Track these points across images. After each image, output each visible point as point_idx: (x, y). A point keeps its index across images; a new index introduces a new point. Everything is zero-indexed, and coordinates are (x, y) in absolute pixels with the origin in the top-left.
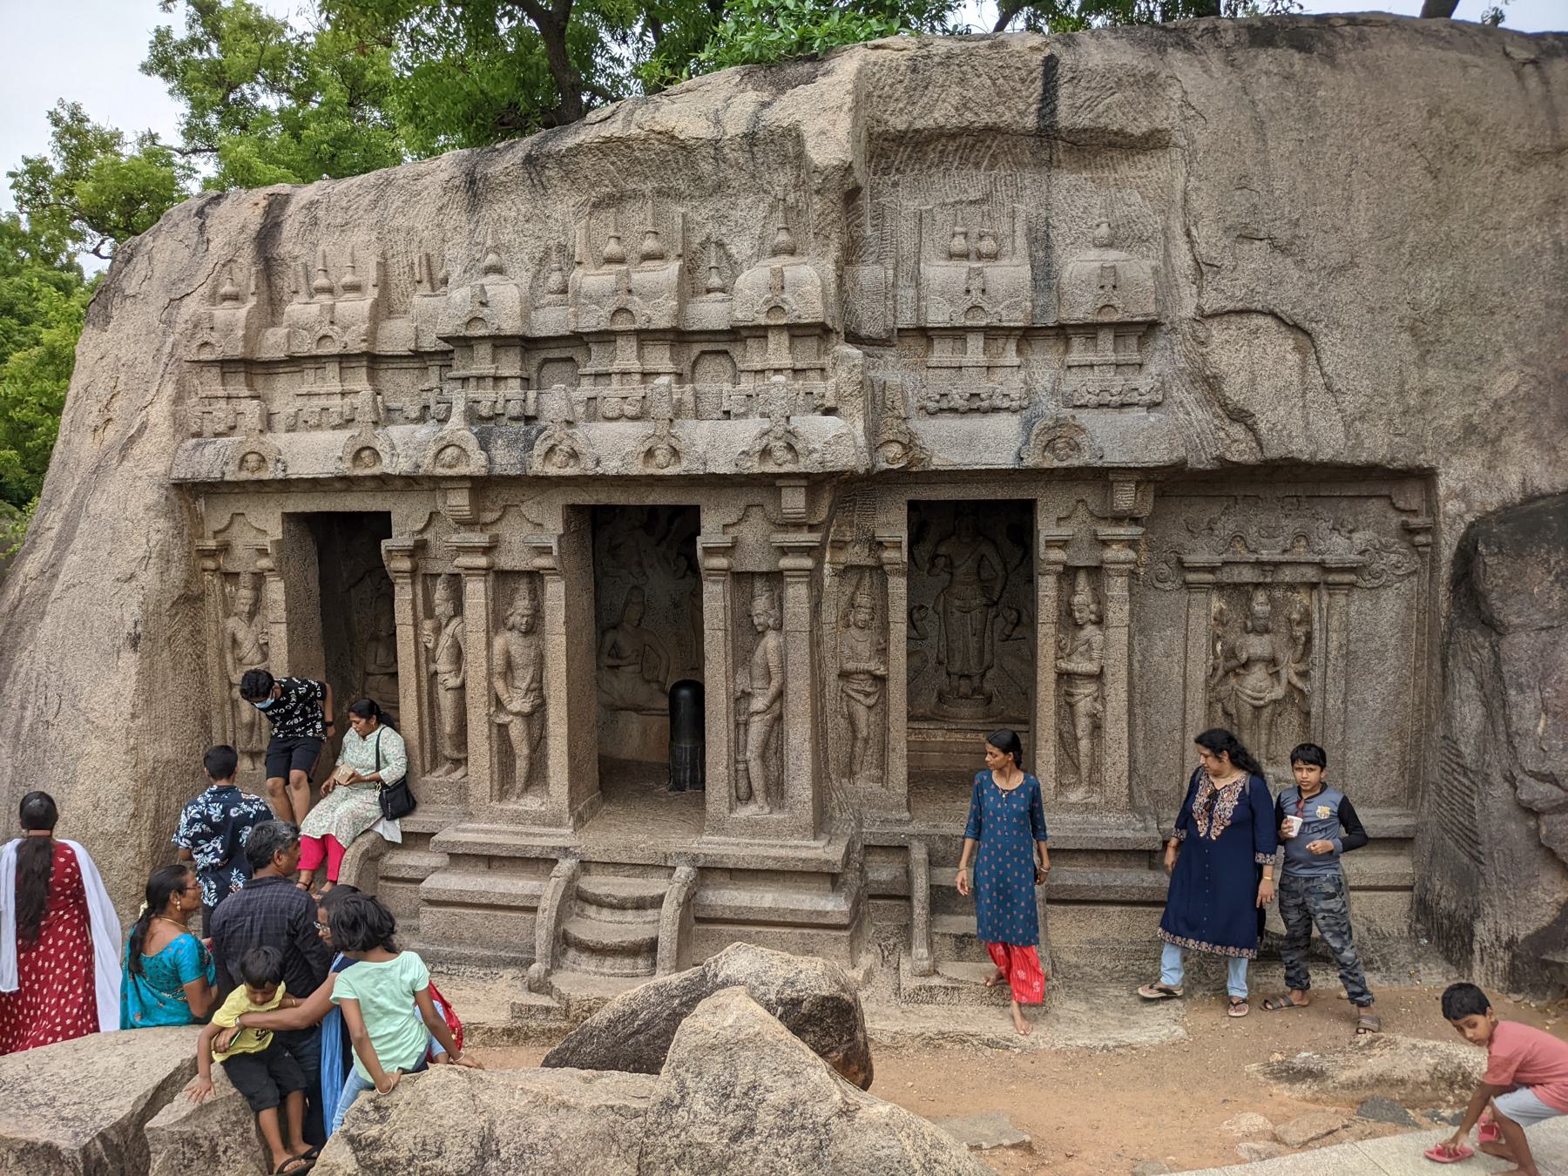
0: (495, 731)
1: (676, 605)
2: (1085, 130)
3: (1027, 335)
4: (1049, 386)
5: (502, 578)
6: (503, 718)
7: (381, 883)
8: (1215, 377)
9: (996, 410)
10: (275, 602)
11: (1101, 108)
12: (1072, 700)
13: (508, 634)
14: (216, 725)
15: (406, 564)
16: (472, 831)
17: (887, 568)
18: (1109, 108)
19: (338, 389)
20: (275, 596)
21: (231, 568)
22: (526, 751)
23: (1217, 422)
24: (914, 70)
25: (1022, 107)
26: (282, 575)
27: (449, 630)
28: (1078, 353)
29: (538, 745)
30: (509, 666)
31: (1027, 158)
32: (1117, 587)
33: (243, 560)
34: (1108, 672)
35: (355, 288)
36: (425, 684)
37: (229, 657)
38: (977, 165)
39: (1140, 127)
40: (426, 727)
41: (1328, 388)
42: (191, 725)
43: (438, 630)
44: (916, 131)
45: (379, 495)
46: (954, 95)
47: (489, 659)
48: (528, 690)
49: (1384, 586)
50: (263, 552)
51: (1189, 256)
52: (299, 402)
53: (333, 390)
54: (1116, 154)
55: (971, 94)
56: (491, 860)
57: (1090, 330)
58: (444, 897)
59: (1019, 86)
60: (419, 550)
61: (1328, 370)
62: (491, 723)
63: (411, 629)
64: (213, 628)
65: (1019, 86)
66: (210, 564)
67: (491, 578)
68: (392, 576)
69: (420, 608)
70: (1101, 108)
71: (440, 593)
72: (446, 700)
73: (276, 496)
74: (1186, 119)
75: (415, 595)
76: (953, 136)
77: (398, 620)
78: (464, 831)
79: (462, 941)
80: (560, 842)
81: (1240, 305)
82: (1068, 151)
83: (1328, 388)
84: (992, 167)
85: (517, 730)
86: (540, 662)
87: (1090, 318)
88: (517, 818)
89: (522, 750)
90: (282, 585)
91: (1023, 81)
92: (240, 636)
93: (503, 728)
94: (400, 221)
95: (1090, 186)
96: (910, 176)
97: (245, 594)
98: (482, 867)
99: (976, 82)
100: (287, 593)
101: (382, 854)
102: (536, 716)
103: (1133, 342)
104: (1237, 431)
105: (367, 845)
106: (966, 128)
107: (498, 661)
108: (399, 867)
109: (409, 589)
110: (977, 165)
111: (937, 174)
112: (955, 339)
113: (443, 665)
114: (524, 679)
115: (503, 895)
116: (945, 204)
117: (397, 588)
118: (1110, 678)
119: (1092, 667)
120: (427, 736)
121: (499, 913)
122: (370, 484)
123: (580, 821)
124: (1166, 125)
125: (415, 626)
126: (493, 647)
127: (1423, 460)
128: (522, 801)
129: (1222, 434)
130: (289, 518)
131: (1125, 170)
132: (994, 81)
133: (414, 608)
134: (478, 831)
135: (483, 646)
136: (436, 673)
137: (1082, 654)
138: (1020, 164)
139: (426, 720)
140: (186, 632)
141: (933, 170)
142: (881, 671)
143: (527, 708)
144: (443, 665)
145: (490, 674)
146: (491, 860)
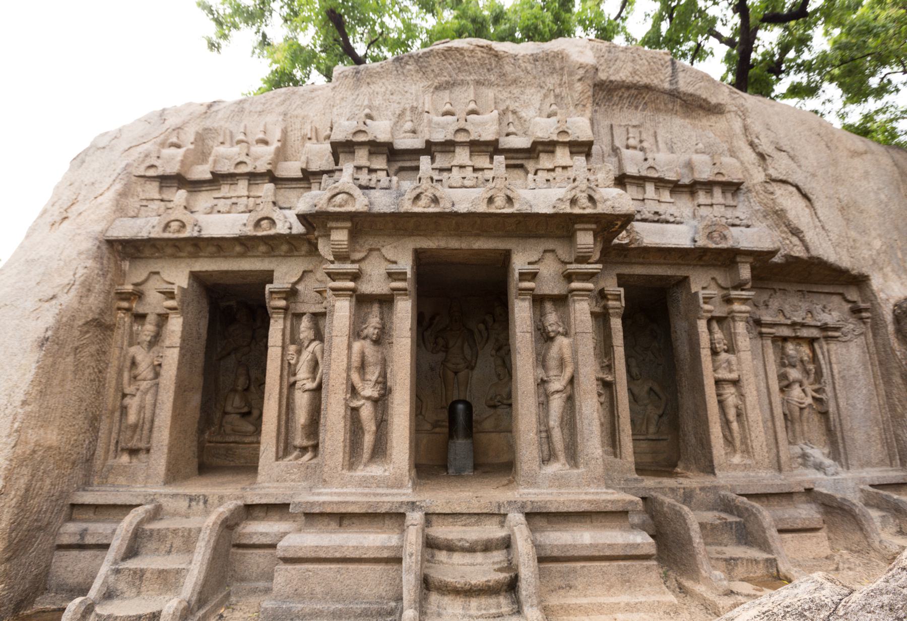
0: (349, 413)
1: (432, 369)
2: (691, 95)
3: (675, 187)
4: (691, 215)
5: (362, 301)
6: (355, 403)
7: (233, 550)
8: (782, 210)
9: (667, 222)
10: (173, 332)
11: (697, 86)
12: (722, 398)
13: (363, 342)
14: (104, 426)
15: (282, 303)
16: (327, 494)
17: (611, 311)
18: (700, 88)
19: (246, 193)
20: (173, 328)
21: (141, 310)
22: (374, 428)
23: (783, 235)
24: (610, 52)
25: (662, 78)
26: (183, 313)
27: (311, 348)
28: (702, 198)
29: (382, 424)
30: (362, 367)
31: (662, 107)
32: (741, 328)
33: (154, 302)
34: (744, 378)
35: (265, 142)
36: (285, 391)
37: (126, 375)
38: (636, 108)
39: (713, 101)
40: (283, 423)
41: (823, 228)
42: (81, 422)
43: (299, 352)
44: (611, 82)
45: (267, 260)
46: (629, 67)
47: (349, 357)
48: (377, 382)
49: (850, 341)
50: (170, 295)
51: (754, 155)
52: (216, 201)
53: (242, 194)
54: (701, 112)
55: (638, 67)
56: (342, 518)
57: (709, 186)
58: (300, 554)
59: (660, 67)
60: (291, 294)
61: (822, 218)
62: (347, 406)
63: (280, 349)
64: (117, 351)
65: (660, 67)
66: (125, 304)
67: (354, 299)
68: (270, 311)
69: (288, 336)
70: (697, 86)
71: (305, 323)
72: (302, 400)
73: (188, 260)
74: (734, 99)
75: (285, 327)
76: (628, 88)
77: (270, 343)
78: (319, 494)
79: (312, 596)
80: (404, 499)
81: (784, 178)
82: (681, 106)
83: (823, 228)
84: (644, 110)
85: (366, 412)
86: (384, 364)
87: (711, 178)
88: (364, 482)
89: (370, 426)
90: (181, 320)
91: (662, 65)
92: (139, 358)
93: (355, 410)
94: (299, 111)
95: (689, 126)
96: (603, 108)
97: (149, 328)
98: (334, 525)
99: (640, 62)
100: (185, 325)
101: (237, 524)
102: (381, 402)
103: (729, 195)
104: (795, 240)
105: (227, 514)
106: (635, 85)
107: (356, 358)
108: (251, 535)
109: (281, 321)
110: (636, 108)
111: (617, 111)
112: (638, 185)
113: (303, 373)
114: (373, 374)
115: (356, 548)
116: (620, 126)
117: (272, 321)
118: (745, 383)
119: (734, 376)
120: (283, 430)
121: (351, 567)
122: (263, 248)
123: (415, 485)
124: (723, 102)
125: (284, 348)
126: (346, 355)
127: (865, 271)
128: (368, 469)
129: (788, 242)
130: (195, 276)
131: (705, 122)
132: (649, 63)
133: (284, 335)
134: (331, 494)
135: (345, 346)
136: (295, 383)
137: (725, 368)
138: (658, 110)
139: (284, 417)
140: (93, 348)
141: (615, 107)
142: (609, 378)
143: (376, 394)
144: (303, 373)
145: (349, 369)
146: (342, 518)
